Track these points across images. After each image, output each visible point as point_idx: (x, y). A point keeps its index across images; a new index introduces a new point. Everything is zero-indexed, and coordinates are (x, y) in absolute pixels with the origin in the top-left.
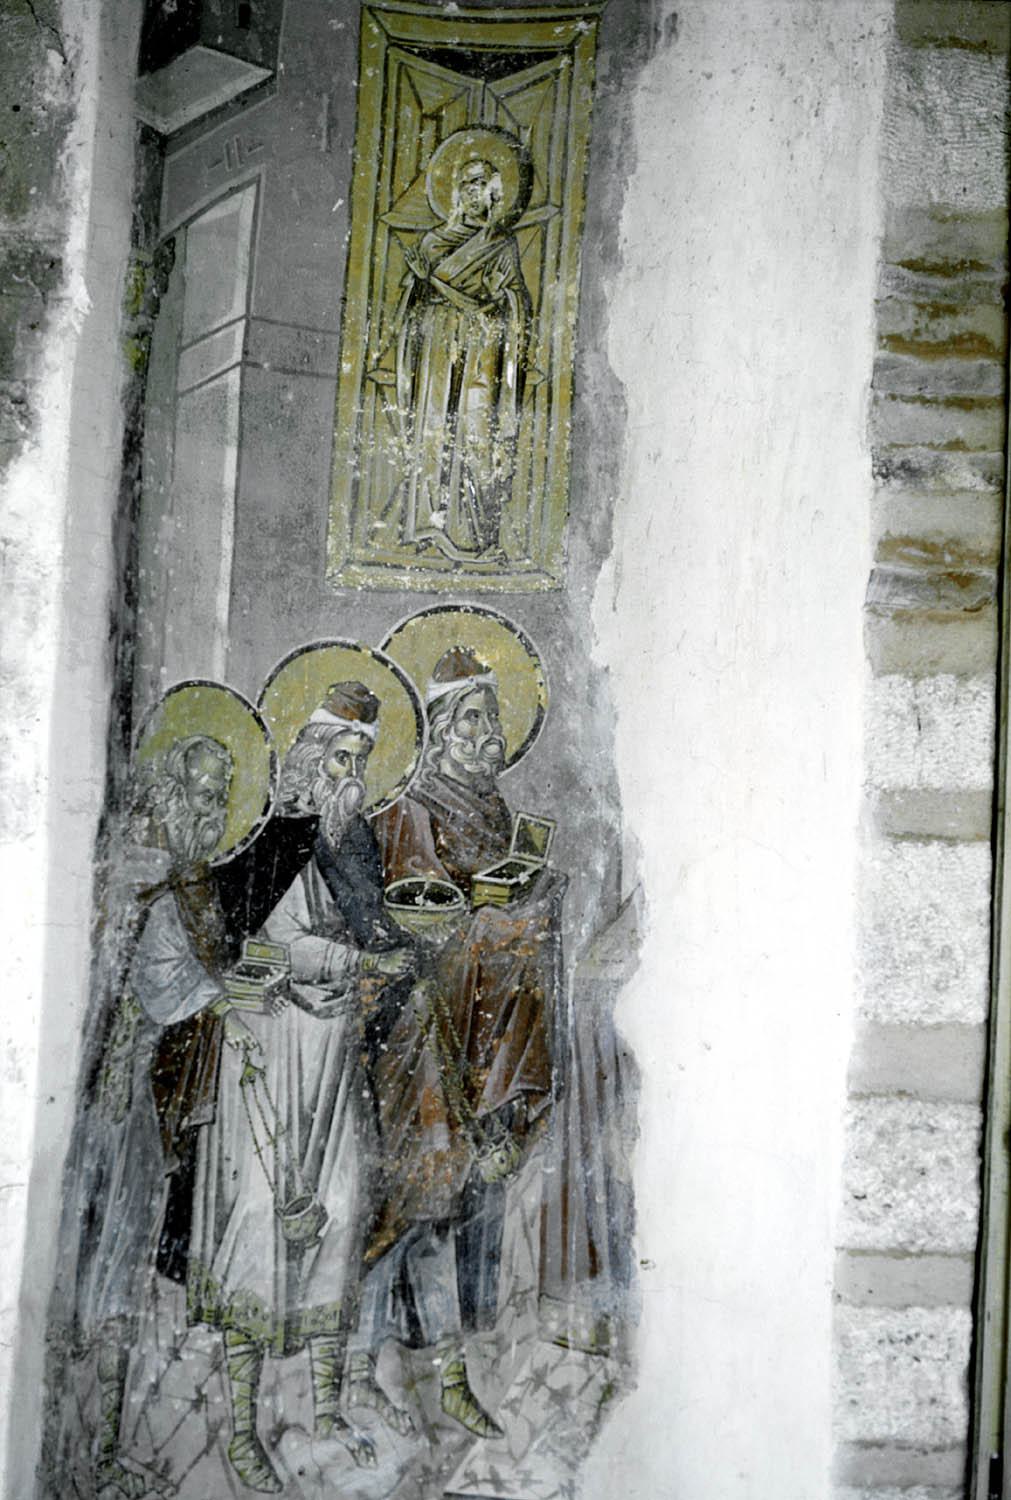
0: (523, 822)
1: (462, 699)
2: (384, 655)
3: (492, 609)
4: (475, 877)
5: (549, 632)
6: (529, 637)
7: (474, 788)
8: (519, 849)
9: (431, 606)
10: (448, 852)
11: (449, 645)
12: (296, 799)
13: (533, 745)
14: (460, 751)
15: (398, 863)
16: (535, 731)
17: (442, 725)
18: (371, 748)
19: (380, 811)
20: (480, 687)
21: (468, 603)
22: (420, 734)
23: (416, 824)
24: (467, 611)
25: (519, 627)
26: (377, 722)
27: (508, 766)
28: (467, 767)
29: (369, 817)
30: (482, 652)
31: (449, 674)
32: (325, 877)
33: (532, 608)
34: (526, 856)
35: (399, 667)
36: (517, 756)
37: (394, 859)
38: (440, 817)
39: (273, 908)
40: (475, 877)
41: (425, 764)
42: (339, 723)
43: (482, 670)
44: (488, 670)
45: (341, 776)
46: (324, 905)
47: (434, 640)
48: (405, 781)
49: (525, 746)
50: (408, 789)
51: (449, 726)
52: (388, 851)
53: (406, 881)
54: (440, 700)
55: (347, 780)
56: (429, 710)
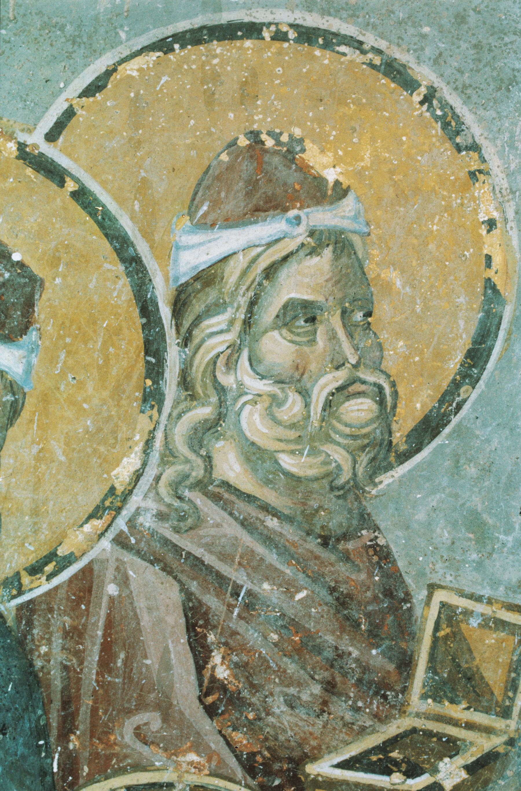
0: (448, 614)
1: (271, 272)
2: (52, 152)
3: (348, 29)
4: (313, 769)
6: (454, 100)
7: (305, 519)
8: (436, 692)
10: (235, 701)
11: (233, 126)
13: (472, 395)
14: (269, 417)
15: (99, 731)
16: (477, 356)
17: (217, 345)
19: (41, 587)
20: (321, 240)
21: (284, 17)
22: (155, 371)
23: (146, 621)
24: (280, 37)
25: (425, 74)
26: (33, 335)
27: (404, 457)
28: (287, 462)
31: (234, 203)
34: (458, 711)
35: (93, 186)
36: (429, 428)
38: (211, 601)
40: (313, 769)
41: (169, 455)
44: (341, 192)
47: (193, 118)
48: (113, 502)
49: (449, 400)
51: (235, 349)
54: (207, 277)
56: (179, 306)
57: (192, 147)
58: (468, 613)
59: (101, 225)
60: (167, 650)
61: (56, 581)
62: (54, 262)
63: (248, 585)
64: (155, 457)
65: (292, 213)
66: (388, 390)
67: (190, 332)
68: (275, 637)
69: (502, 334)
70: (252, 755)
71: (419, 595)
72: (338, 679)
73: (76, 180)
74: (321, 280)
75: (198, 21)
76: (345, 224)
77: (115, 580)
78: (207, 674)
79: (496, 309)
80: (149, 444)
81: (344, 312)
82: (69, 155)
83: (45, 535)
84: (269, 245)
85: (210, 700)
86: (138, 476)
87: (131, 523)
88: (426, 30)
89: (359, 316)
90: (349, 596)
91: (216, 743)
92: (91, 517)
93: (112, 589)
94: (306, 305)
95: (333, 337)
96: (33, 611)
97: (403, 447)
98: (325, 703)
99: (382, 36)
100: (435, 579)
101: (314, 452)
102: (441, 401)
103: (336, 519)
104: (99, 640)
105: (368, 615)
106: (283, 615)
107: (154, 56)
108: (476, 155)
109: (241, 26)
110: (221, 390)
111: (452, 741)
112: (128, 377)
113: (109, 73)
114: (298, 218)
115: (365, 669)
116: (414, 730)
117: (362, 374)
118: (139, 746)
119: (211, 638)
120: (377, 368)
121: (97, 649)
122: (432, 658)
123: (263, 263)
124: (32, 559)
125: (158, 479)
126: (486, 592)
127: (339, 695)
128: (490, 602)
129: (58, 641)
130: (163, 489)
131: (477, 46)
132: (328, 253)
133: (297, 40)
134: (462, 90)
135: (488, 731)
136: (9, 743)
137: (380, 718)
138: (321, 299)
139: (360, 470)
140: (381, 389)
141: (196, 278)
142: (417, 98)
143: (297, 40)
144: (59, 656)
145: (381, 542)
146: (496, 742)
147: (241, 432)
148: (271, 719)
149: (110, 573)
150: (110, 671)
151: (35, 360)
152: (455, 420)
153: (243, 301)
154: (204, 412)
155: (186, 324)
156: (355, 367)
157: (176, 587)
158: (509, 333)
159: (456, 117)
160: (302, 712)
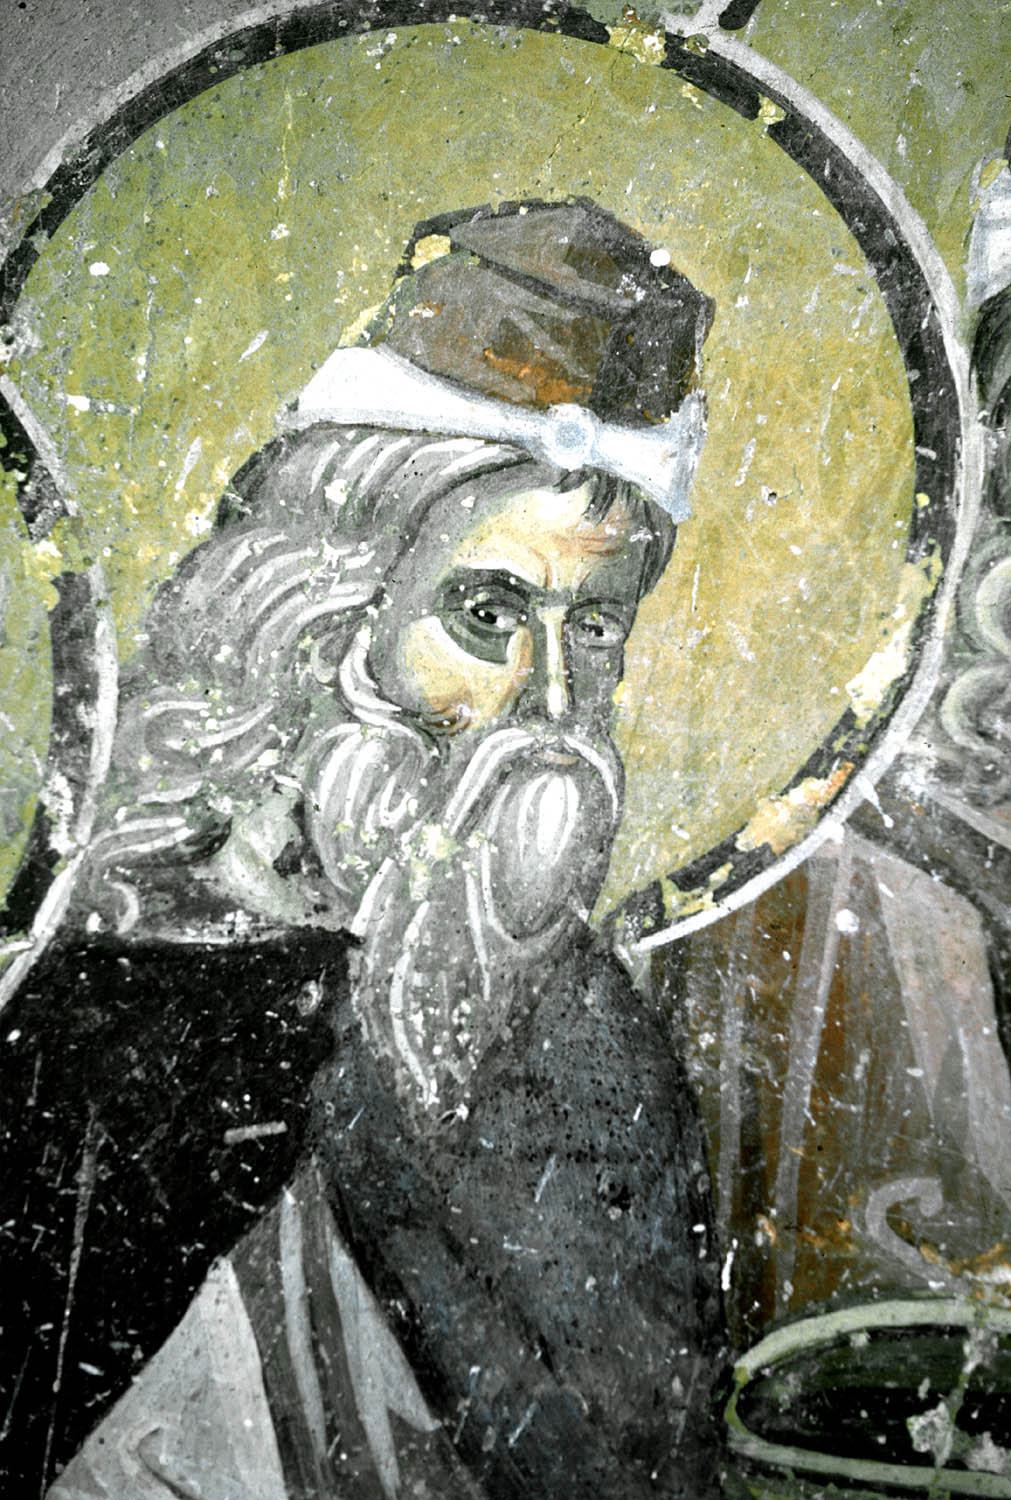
12: (211, 840)
15: (815, 1212)
18: (654, 562)
19: (703, 914)
23: (912, 986)
26: (691, 410)
29: (637, 952)
32: (381, 1279)
39: (67, 1449)
42: (469, 423)
45: (479, 714)
46: (379, 1435)
48: (847, 744)
50: (865, 788)
53: (855, 1320)
55: (516, 739)
59: (829, 189)
60: (955, 1050)
62: (736, 264)
77: (850, 903)
83: (712, 808)
86: (900, 690)
87: (885, 786)
92: (803, 774)
93: (845, 921)
96: (685, 962)
104: (818, 1025)
118: (896, 1246)
121: (813, 1043)
124: (685, 857)
129: (735, 1026)
136: (633, 1225)
144: (737, 1055)
149: (841, 889)
150: (840, 1090)
151: (693, 460)
157: (975, 917)
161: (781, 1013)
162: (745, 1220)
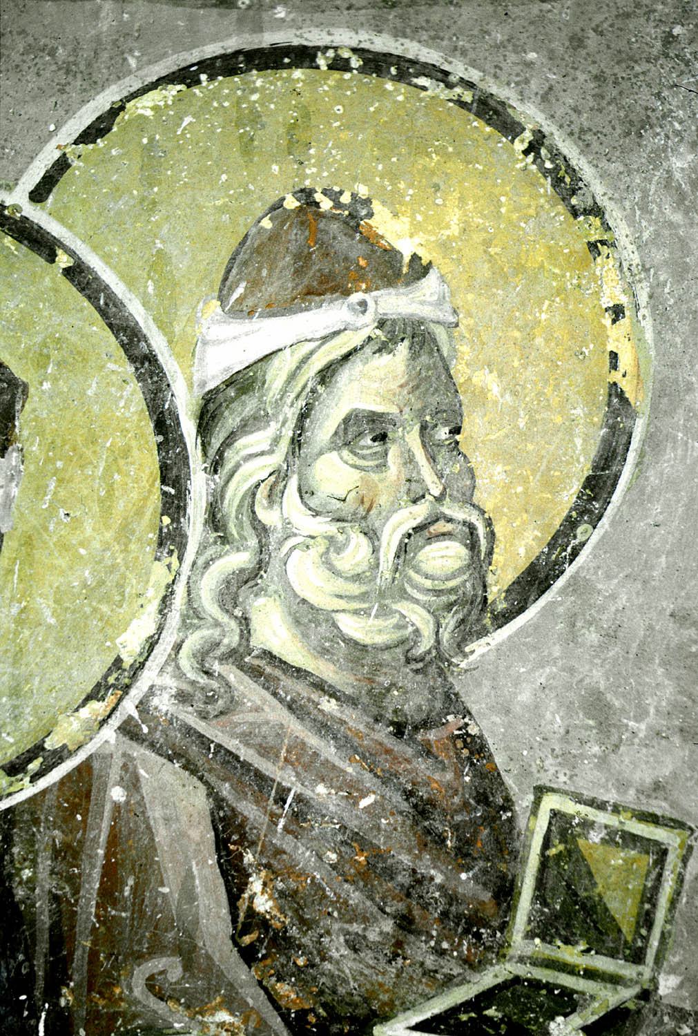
0: (561, 825)
1: (327, 375)
2: (37, 215)
3: (430, 55)
5: (637, 127)
6: (569, 149)
7: (373, 700)
8: (544, 929)
9: (211, 50)
10: (281, 942)
11: (277, 182)
13: (592, 537)
16: (598, 486)
20: (393, 333)
21: (345, 38)
22: (174, 505)
23: (162, 835)
24: (339, 65)
25: (530, 114)
27: (503, 619)
30: (394, 202)
31: (279, 284)
33: (577, 42)
35: (93, 261)
36: (535, 580)
37: (78, 974)
38: (249, 809)
41: (193, 616)
43: (393, 270)
44: (420, 269)
48: (118, 679)
50: (129, 707)
51: (280, 476)
52: (61, 938)
54: (244, 382)
56: (207, 419)
57: (222, 210)
58: (587, 825)
59: (103, 313)
60: (189, 876)
61: (43, 783)
62: (42, 360)
63: (297, 789)
64: (174, 619)
65: (356, 297)
66: (481, 531)
67: (220, 453)
68: (333, 857)
69: (631, 456)
70: (302, 1014)
71: (524, 802)
72: (416, 912)
73: (71, 253)
74: (394, 386)
75: (232, 44)
76: (427, 312)
77: (121, 782)
78: (243, 906)
79: (623, 423)
80: (166, 601)
81: (423, 428)
82: (62, 220)
83: (29, 721)
84: (325, 339)
85: (247, 940)
86: (152, 644)
87: (142, 706)
88: (532, 56)
89: (443, 433)
90: (431, 802)
91: (254, 998)
92: (89, 698)
93: (117, 794)
94: (374, 418)
95: (410, 460)
96: (12, 823)
97: (502, 606)
98: (399, 944)
99: (473, 64)
100: (544, 780)
101: (384, 612)
102: (552, 545)
103: (413, 698)
104: (100, 862)
105: (456, 828)
106: (344, 828)
107: (174, 89)
108: (597, 222)
109: (288, 50)
110: (262, 530)
111: (567, 993)
112: (139, 513)
113: (115, 111)
114: (363, 304)
115: (452, 899)
116: (517, 980)
117: (448, 509)
118: (153, 1003)
119: (249, 858)
120: (468, 500)
121: (96, 873)
122: (540, 884)
123: (318, 362)
125: (178, 647)
126: (611, 796)
127: (418, 933)
128: (616, 810)
129: (45, 863)
130: (185, 661)
131: (599, 78)
132: (403, 349)
133: (361, 70)
134: (579, 136)
135: (614, 980)
137: (473, 965)
138: (394, 410)
139: (445, 636)
140: (472, 529)
141: (229, 383)
142: (519, 146)
143: (361, 70)
144: (47, 882)
145: (473, 730)
146: (626, 994)
147: (288, 586)
148: (327, 966)
149: (115, 773)
150: (114, 903)
151: (15, 491)
152: (570, 570)
153: (291, 413)
154: (239, 559)
155: (216, 443)
156: (439, 499)
158: (642, 455)
159: (571, 170)
160: (368, 956)
161: (76, 854)
162: (52, 993)
